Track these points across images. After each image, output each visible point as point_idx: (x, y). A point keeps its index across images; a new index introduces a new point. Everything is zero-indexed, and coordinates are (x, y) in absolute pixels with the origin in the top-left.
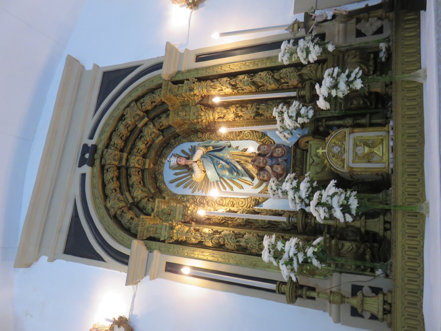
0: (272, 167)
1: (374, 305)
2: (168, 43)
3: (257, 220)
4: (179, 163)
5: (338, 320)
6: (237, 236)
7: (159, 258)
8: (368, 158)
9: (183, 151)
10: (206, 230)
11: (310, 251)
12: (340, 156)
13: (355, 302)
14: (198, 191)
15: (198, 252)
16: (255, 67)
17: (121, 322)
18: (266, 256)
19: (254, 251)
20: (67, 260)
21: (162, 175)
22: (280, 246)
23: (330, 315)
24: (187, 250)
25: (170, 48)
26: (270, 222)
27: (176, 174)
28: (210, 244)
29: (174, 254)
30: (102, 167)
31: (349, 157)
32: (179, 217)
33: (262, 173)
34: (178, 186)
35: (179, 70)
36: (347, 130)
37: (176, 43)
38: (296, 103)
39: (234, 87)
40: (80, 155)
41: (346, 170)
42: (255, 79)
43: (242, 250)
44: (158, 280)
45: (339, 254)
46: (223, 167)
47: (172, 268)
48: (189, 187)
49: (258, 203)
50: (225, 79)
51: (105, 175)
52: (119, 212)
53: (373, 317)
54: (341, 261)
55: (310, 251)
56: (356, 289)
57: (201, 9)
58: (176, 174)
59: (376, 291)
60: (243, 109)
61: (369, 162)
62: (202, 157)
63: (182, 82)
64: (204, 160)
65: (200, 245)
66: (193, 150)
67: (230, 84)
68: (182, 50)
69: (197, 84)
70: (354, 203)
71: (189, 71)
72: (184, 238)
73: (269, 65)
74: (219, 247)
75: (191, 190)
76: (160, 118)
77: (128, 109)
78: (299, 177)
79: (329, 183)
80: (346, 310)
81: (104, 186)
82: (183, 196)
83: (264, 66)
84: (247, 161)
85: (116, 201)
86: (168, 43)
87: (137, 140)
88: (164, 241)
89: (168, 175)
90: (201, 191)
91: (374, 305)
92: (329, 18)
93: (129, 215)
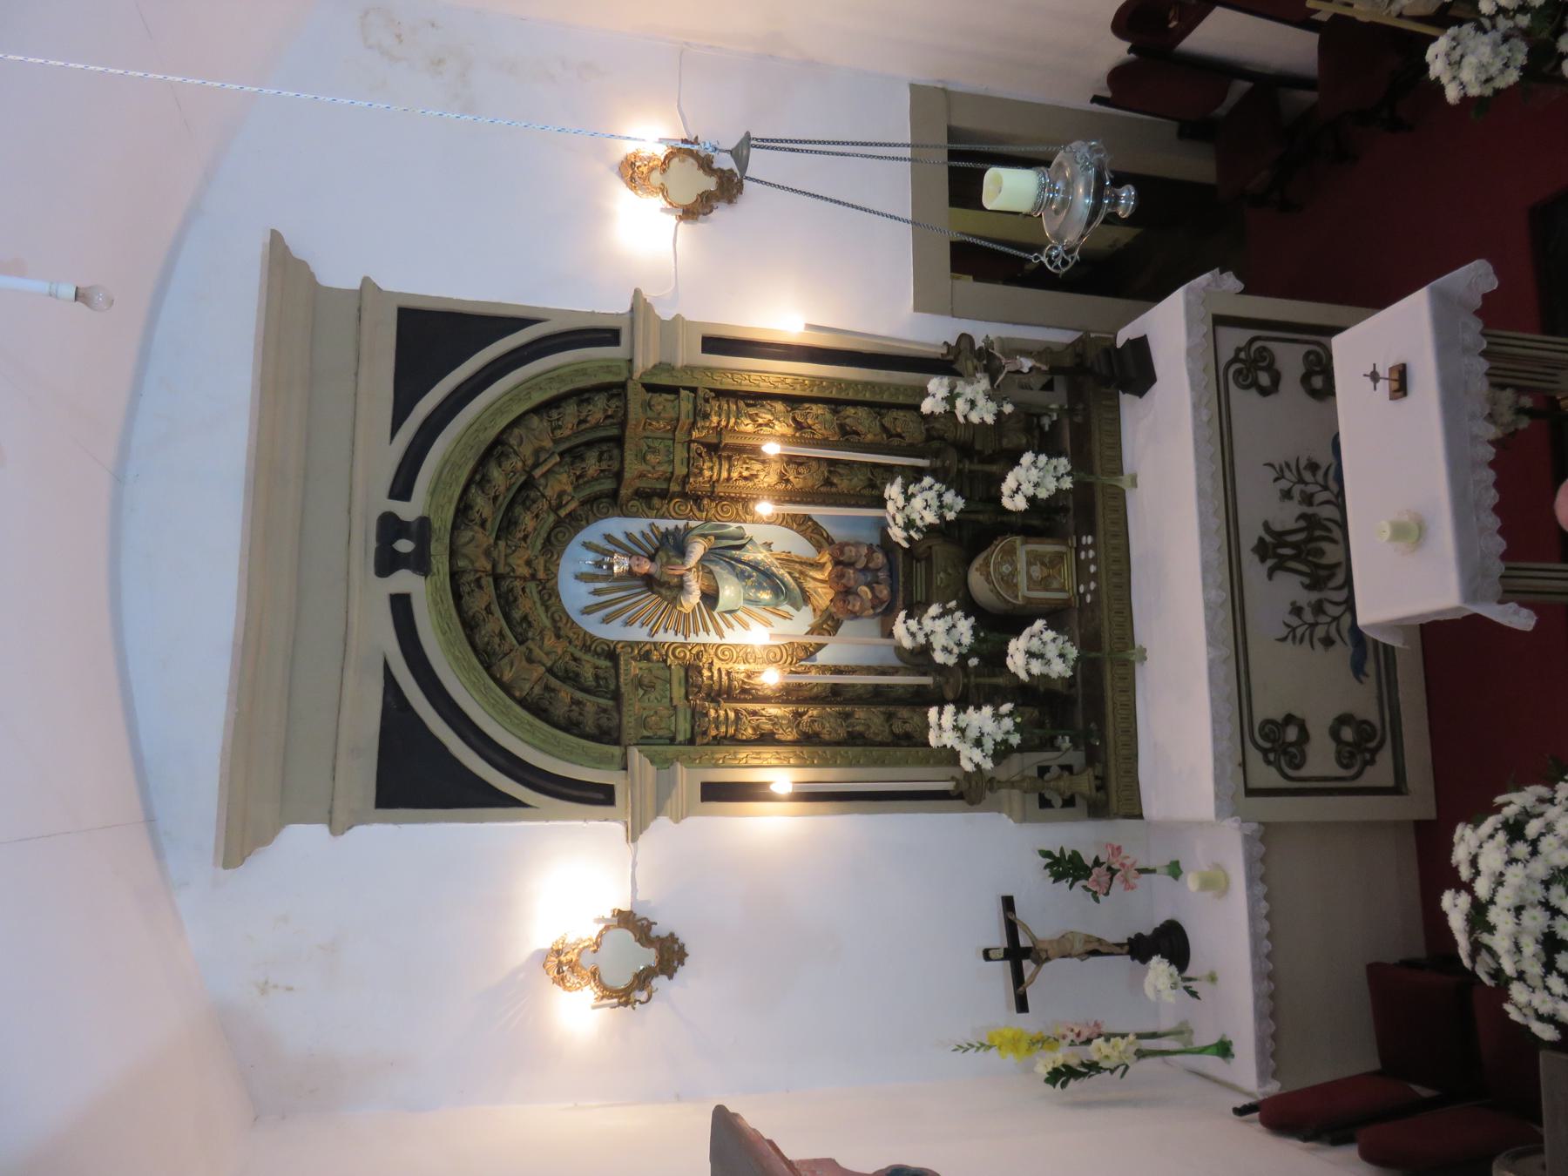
0: (869, 585)
2: (637, 293)
3: (853, 685)
4: (635, 569)
5: (1024, 819)
7: (688, 779)
8: (1044, 584)
9: (608, 538)
10: (773, 710)
12: (1009, 581)
14: (666, 630)
15: (768, 754)
16: (843, 396)
19: (879, 738)
20: (395, 823)
21: (558, 596)
23: (1010, 816)
24: (744, 753)
25: (639, 306)
26: (877, 686)
27: (596, 592)
28: (790, 738)
29: (716, 766)
30: (454, 575)
31: (1022, 580)
33: (851, 598)
34: (606, 620)
35: (664, 360)
36: (1018, 540)
37: (649, 294)
38: (927, 481)
39: (799, 426)
40: (373, 544)
41: (1020, 601)
42: (848, 421)
43: (854, 739)
44: (691, 821)
46: (760, 587)
47: (716, 793)
48: (638, 624)
49: (810, 652)
50: (779, 406)
51: (466, 598)
52: (537, 690)
53: (1069, 802)
56: (1043, 770)
57: (701, 227)
58: (596, 592)
60: (801, 470)
61: (1046, 589)
62: (702, 559)
63: (674, 390)
64: (716, 569)
65: (765, 739)
66: (676, 545)
67: (794, 419)
68: (665, 313)
69: (715, 404)
71: (690, 369)
72: (731, 731)
73: (868, 396)
74: (808, 739)
75: (646, 629)
76: (582, 458)
77: (516, 431)
79: (1031, 623)
80: (1033, 799)
81: (470, 625)
82: (631, 645)
83: (860, 397)
84: (801, 573)
85: (524, 663)
86: (637, 293)
87: (518, 510)
88: (691, 742)
89: (574, 594)
90: (671, 632)
92: (1026, 370)
93: (566, 693)
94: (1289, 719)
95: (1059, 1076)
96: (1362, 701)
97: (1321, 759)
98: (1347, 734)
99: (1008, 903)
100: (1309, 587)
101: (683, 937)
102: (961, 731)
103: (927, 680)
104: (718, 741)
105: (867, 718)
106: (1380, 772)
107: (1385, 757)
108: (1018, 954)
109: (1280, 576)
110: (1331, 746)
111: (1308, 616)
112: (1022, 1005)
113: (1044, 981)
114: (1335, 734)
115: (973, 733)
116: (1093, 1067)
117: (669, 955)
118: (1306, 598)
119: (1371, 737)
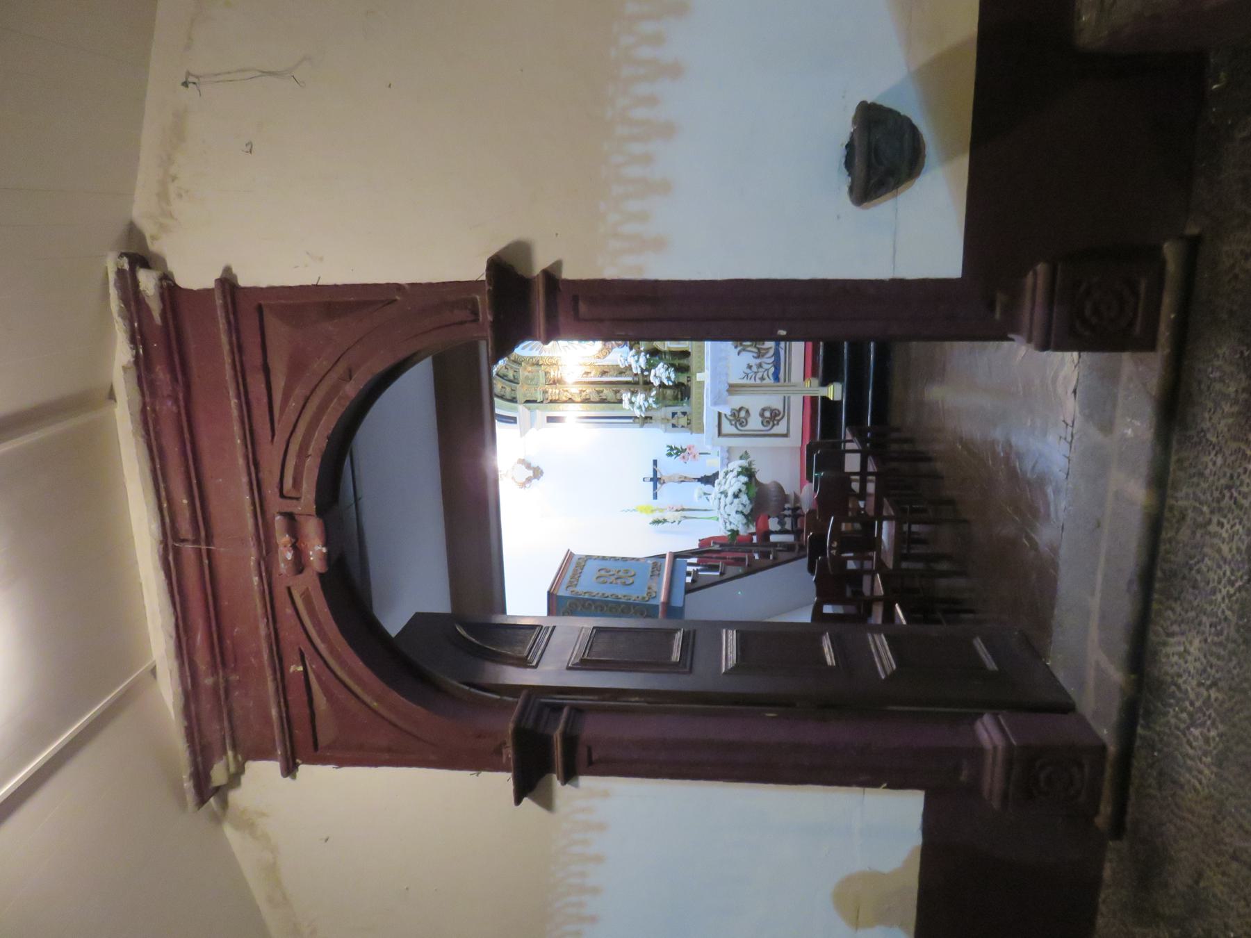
1: (683, 421)
6: (599, 392)
7: (541, 414)
11: (651, 400)
13: (674, 421)
15: (571, 406)
17: (522, 462)
18: (626, 404)
22: (633, 399)
24: (562, 406)
32: (542, 380)
43: (603, 401)
45: (664, 398)
47: (551, 419)
54: (668, 402)
55: (651, 400)
56: (674, 414)
59: (684, 413)
65: (571, 401)
70: (673, 376)
74: (586, 401)
78: (638, 353)
91: (683, 421)
94: (741, 409)
95: (657, 522)
96: (775, 402)
97: (755, 423)
98: (767, 414)
99: (655, 462)
100: (758, 357)
101: (543, 467)
102: (632, 403)
103: (630, 379)
104: (552, 402)
105: (608, 393)
106: (781, 428)
107: (783, 423)
108: (656, 480)
109: (744, 353)
110: (760, 419)
111: (755, 369)
112: (655, 497)
113: (662, 490)
114: (762, 415)
115: (637, 404)
116: (665, 521)
117: (537, 473)
118: (754, 362)
119: (776, 415)
